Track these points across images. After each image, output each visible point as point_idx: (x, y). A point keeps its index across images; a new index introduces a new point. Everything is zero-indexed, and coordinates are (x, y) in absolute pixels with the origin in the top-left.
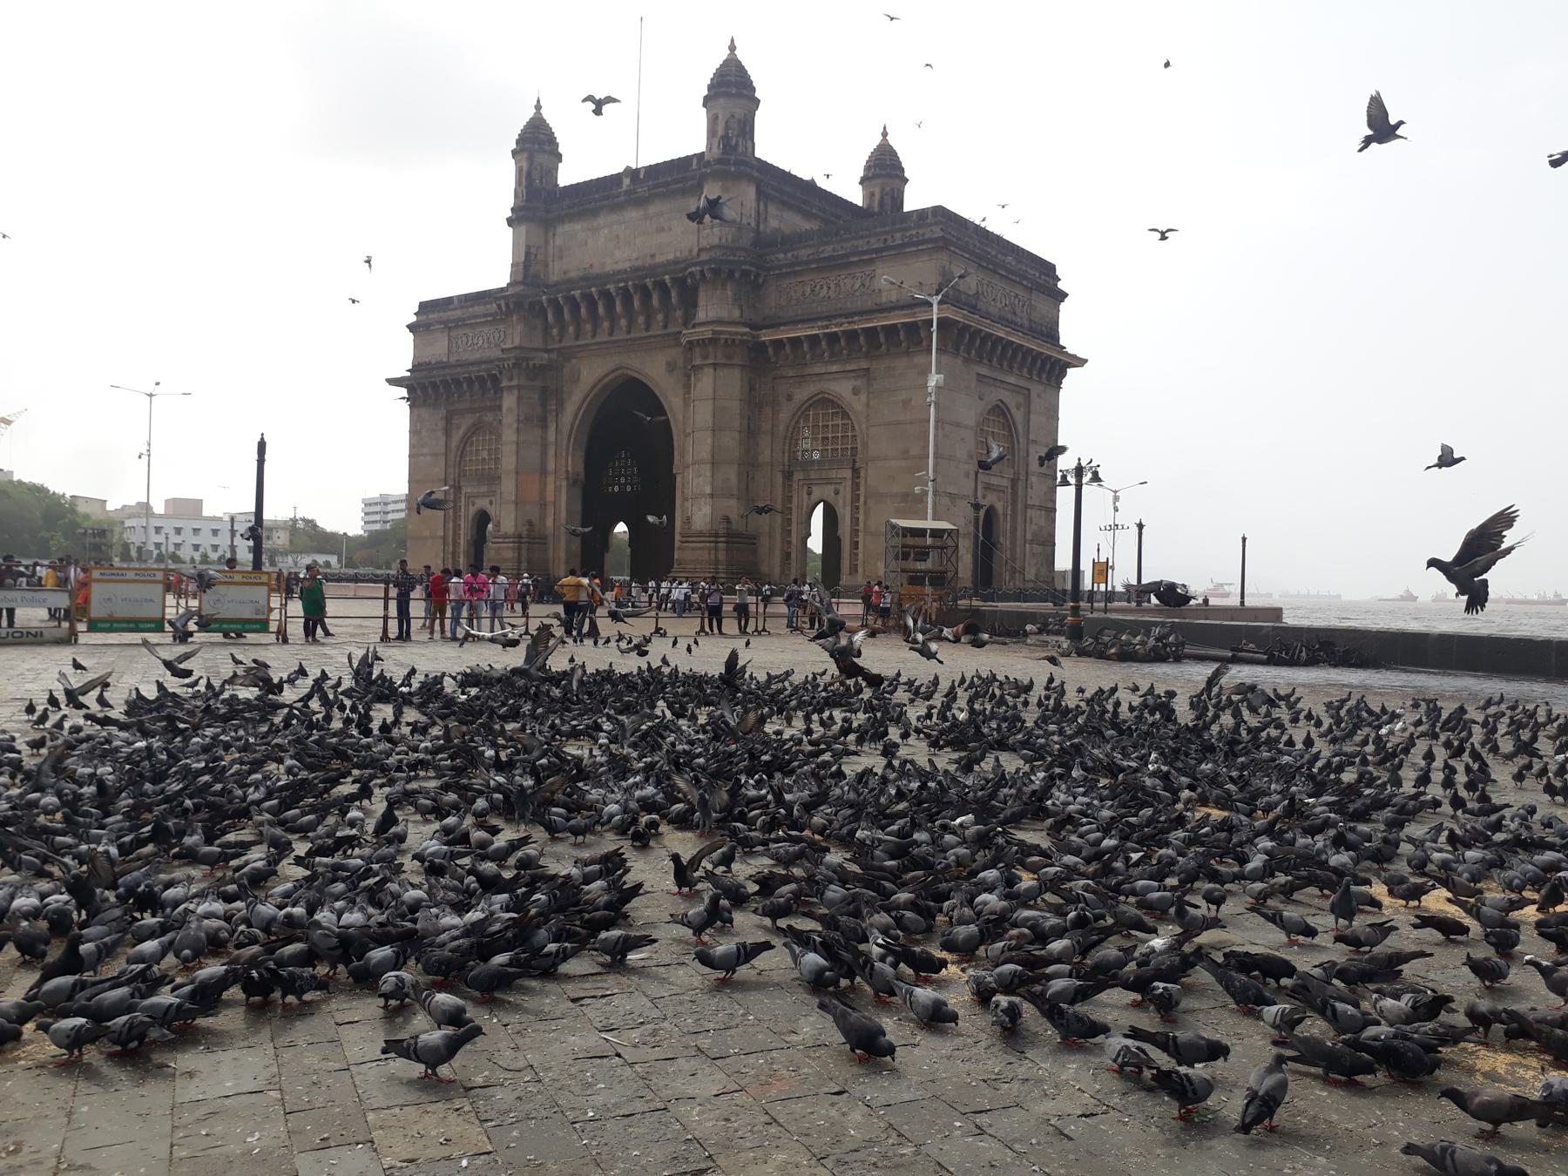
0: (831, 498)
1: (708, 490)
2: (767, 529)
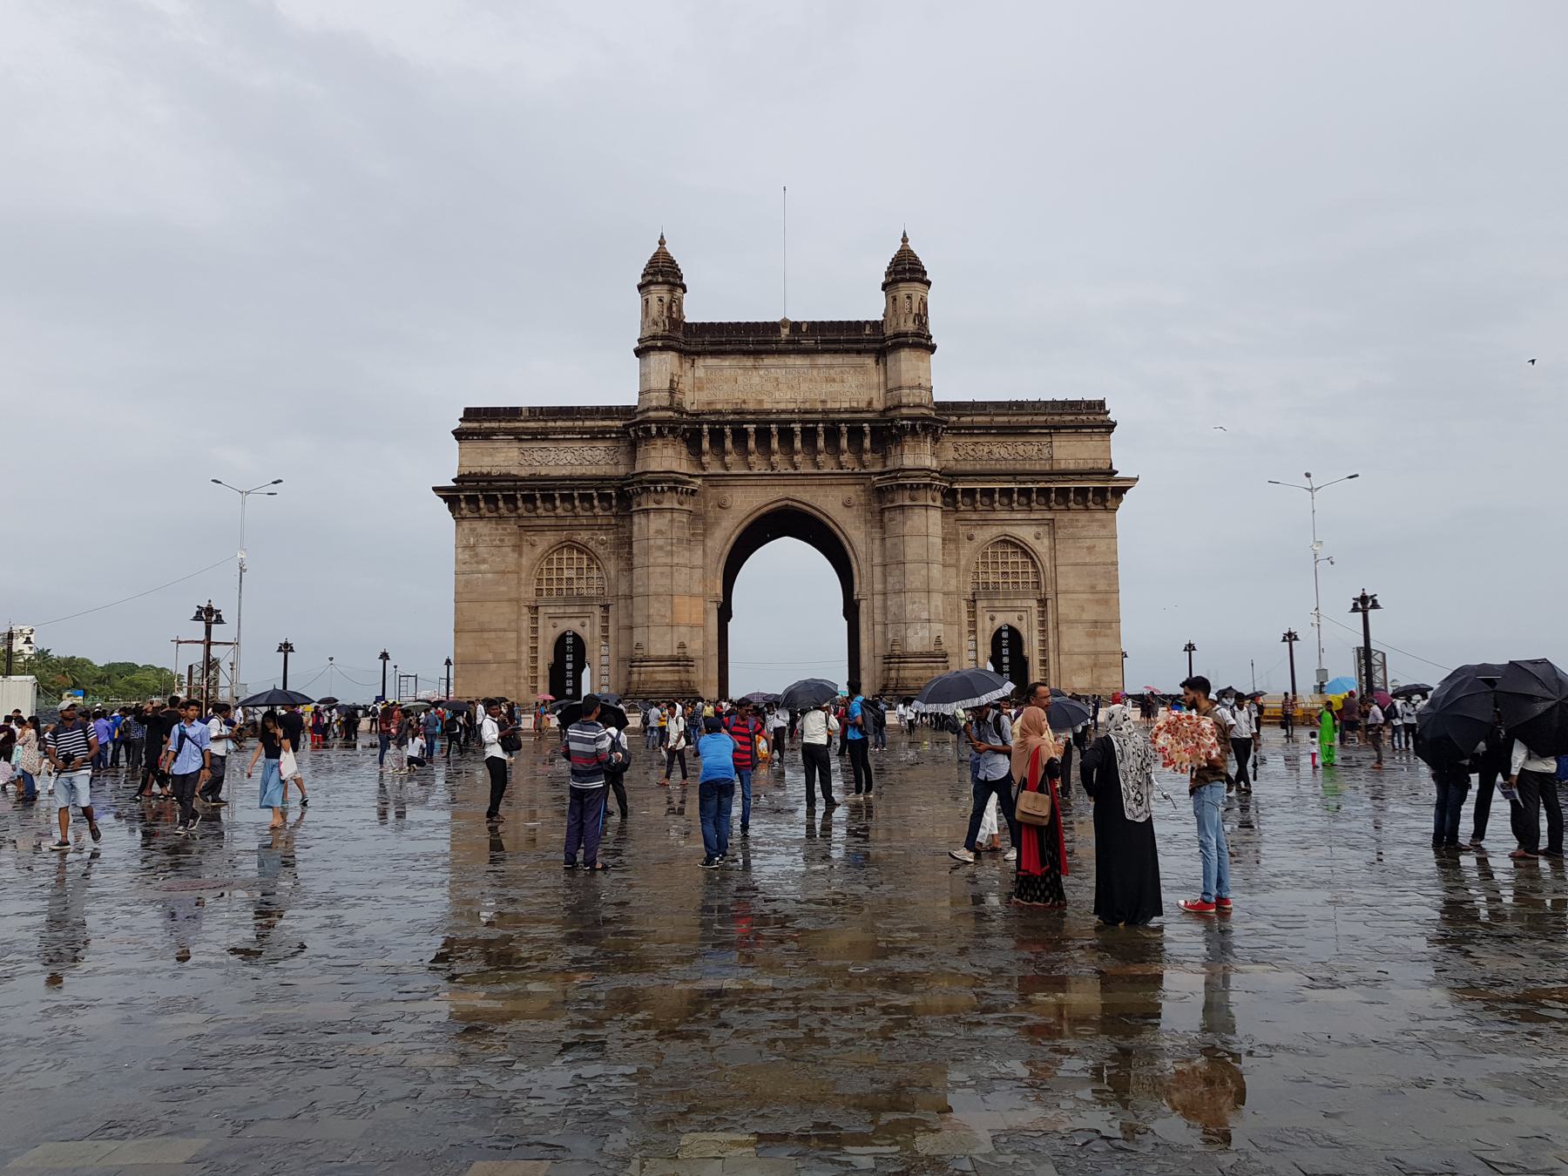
0: (1015, 624)
1: (925, 615)
2: (957, 651)
